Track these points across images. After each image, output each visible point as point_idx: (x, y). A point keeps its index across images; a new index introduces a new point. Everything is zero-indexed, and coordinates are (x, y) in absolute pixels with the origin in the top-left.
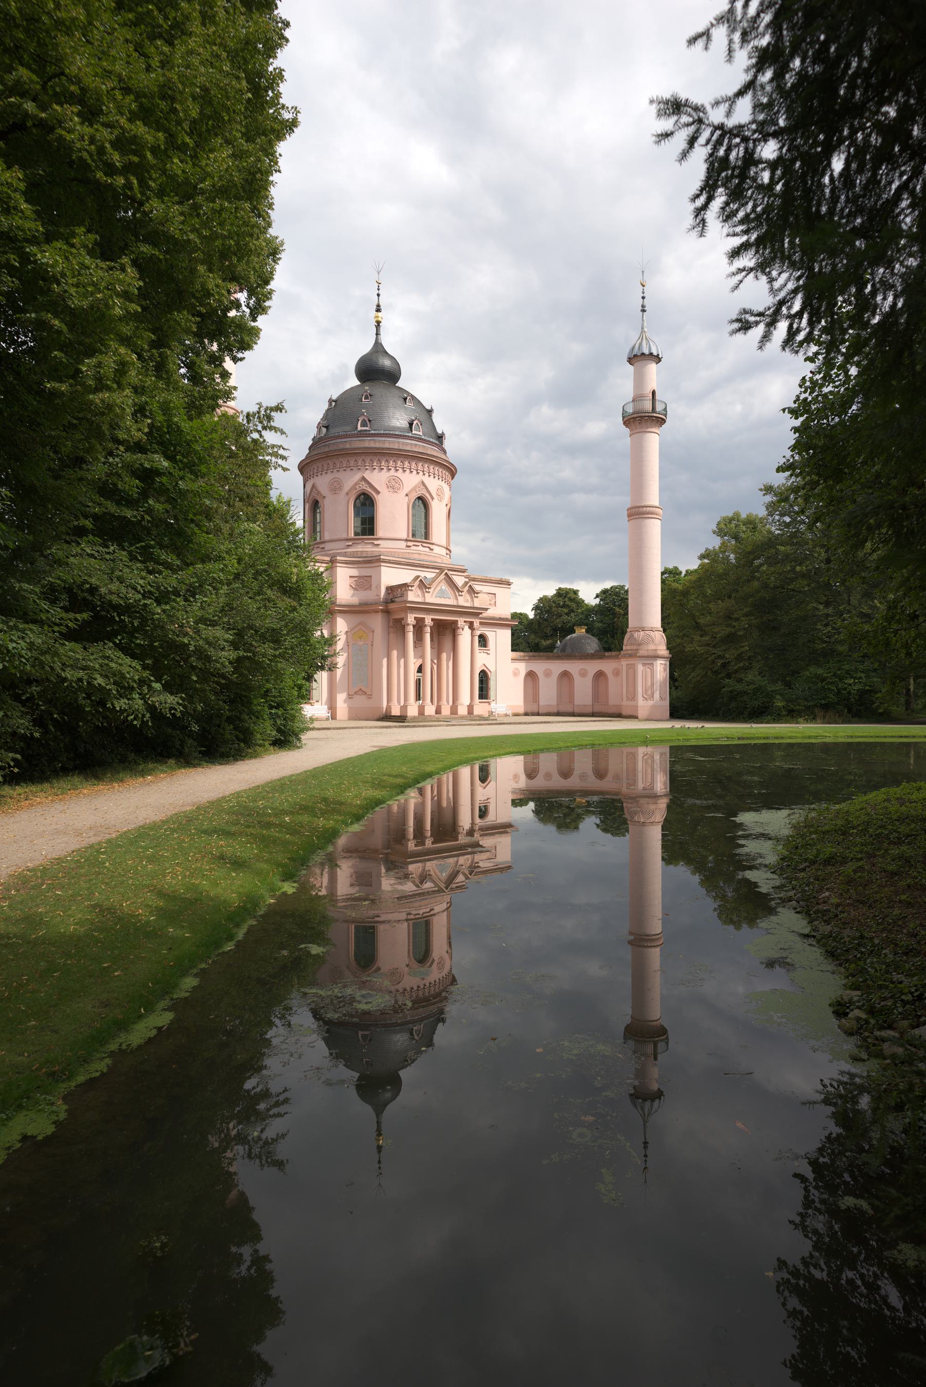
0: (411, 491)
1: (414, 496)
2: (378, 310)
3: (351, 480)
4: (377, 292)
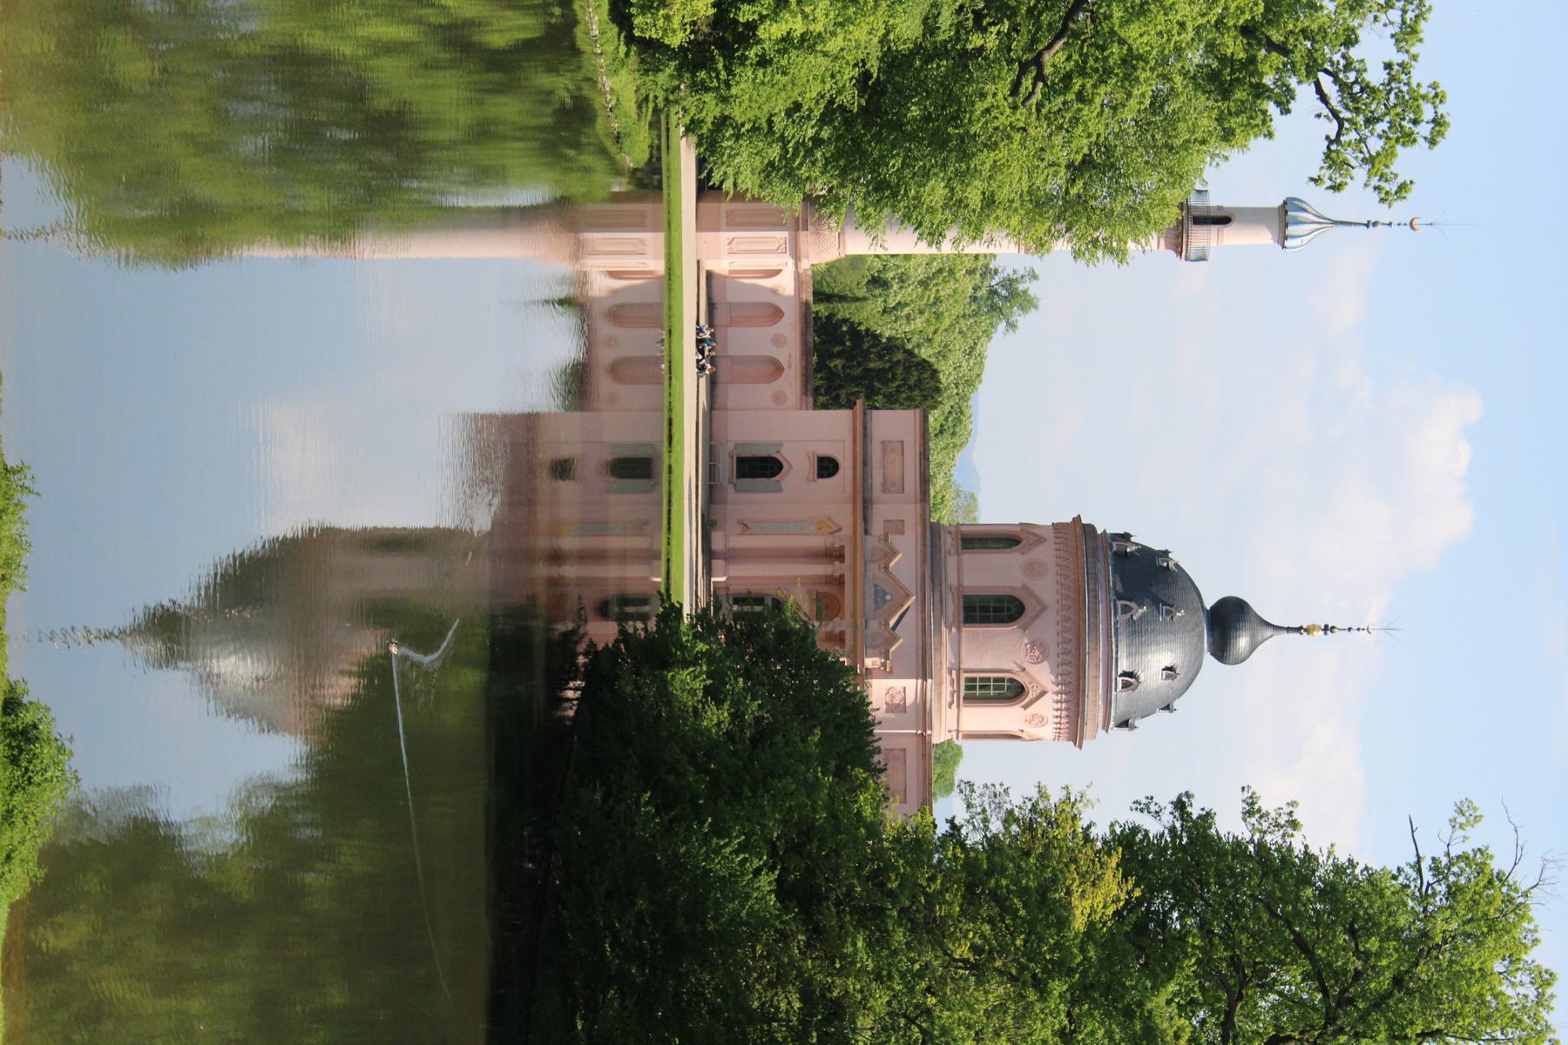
0: (1028, 675)
1: (1022, 679)
2: (1326, 628)
3: (1047, 589)
4: (1355, 627)
